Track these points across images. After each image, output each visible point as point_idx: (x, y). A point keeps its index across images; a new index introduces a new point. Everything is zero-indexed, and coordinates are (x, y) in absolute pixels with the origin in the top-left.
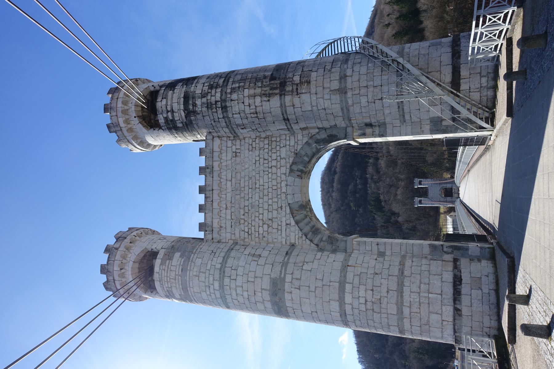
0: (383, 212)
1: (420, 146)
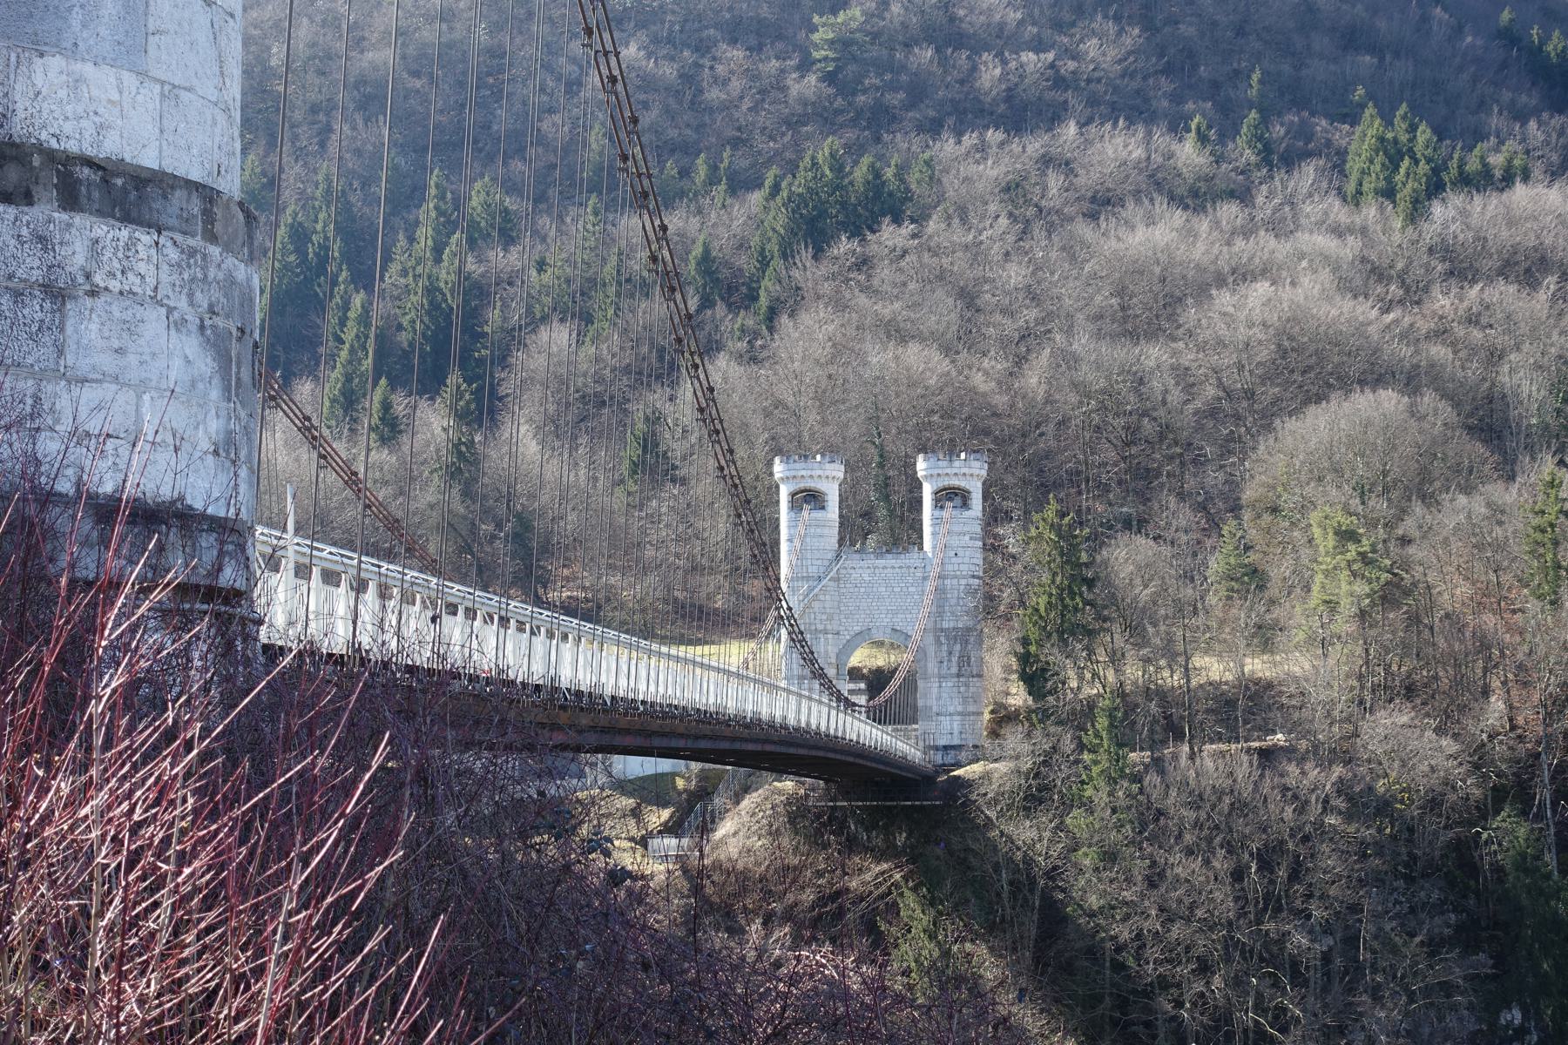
0: (787, 254)
1: (1248, 495)
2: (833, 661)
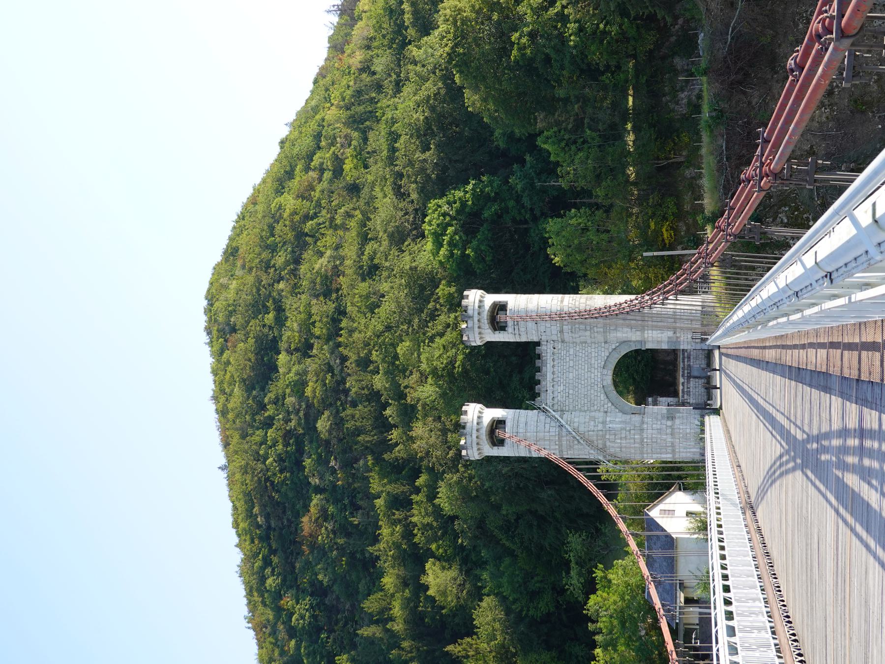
2: (628, 417)
